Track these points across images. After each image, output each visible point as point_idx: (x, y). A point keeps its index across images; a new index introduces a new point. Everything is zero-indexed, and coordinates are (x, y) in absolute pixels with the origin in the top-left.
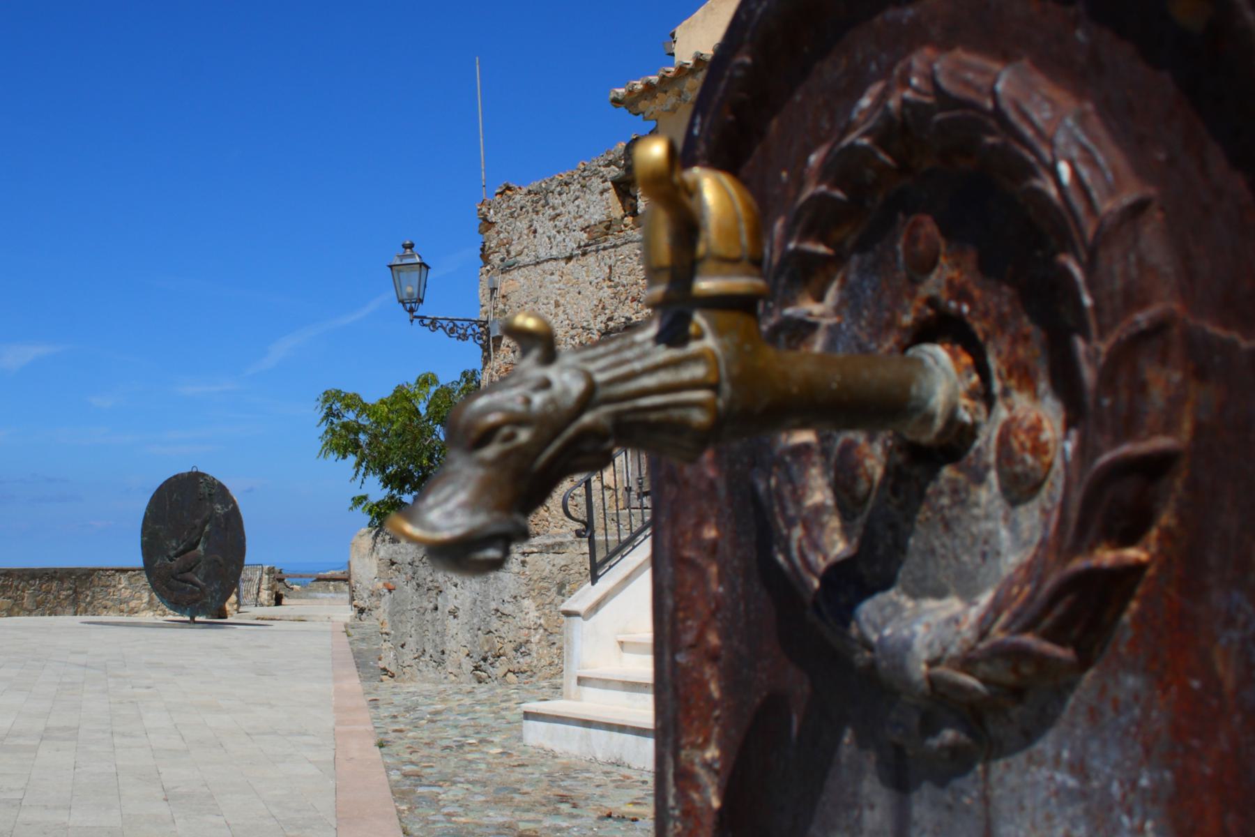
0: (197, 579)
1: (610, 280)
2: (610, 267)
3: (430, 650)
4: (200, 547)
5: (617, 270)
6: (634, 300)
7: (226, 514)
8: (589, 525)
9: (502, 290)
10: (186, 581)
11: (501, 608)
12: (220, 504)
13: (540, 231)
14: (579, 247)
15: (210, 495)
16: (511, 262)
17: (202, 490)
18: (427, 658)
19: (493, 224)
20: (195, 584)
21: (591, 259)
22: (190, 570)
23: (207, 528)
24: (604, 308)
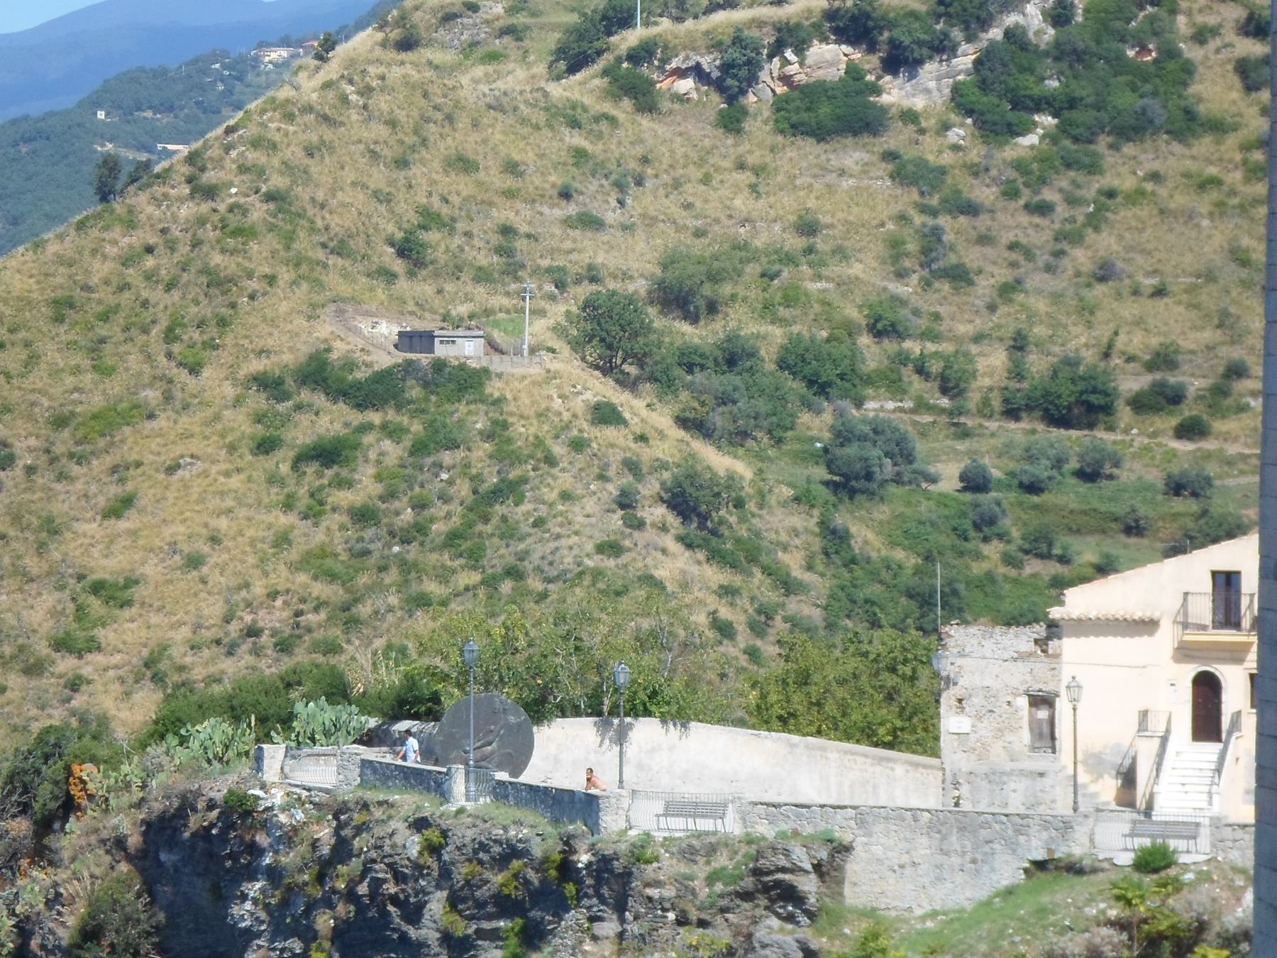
21: (1019, 663)
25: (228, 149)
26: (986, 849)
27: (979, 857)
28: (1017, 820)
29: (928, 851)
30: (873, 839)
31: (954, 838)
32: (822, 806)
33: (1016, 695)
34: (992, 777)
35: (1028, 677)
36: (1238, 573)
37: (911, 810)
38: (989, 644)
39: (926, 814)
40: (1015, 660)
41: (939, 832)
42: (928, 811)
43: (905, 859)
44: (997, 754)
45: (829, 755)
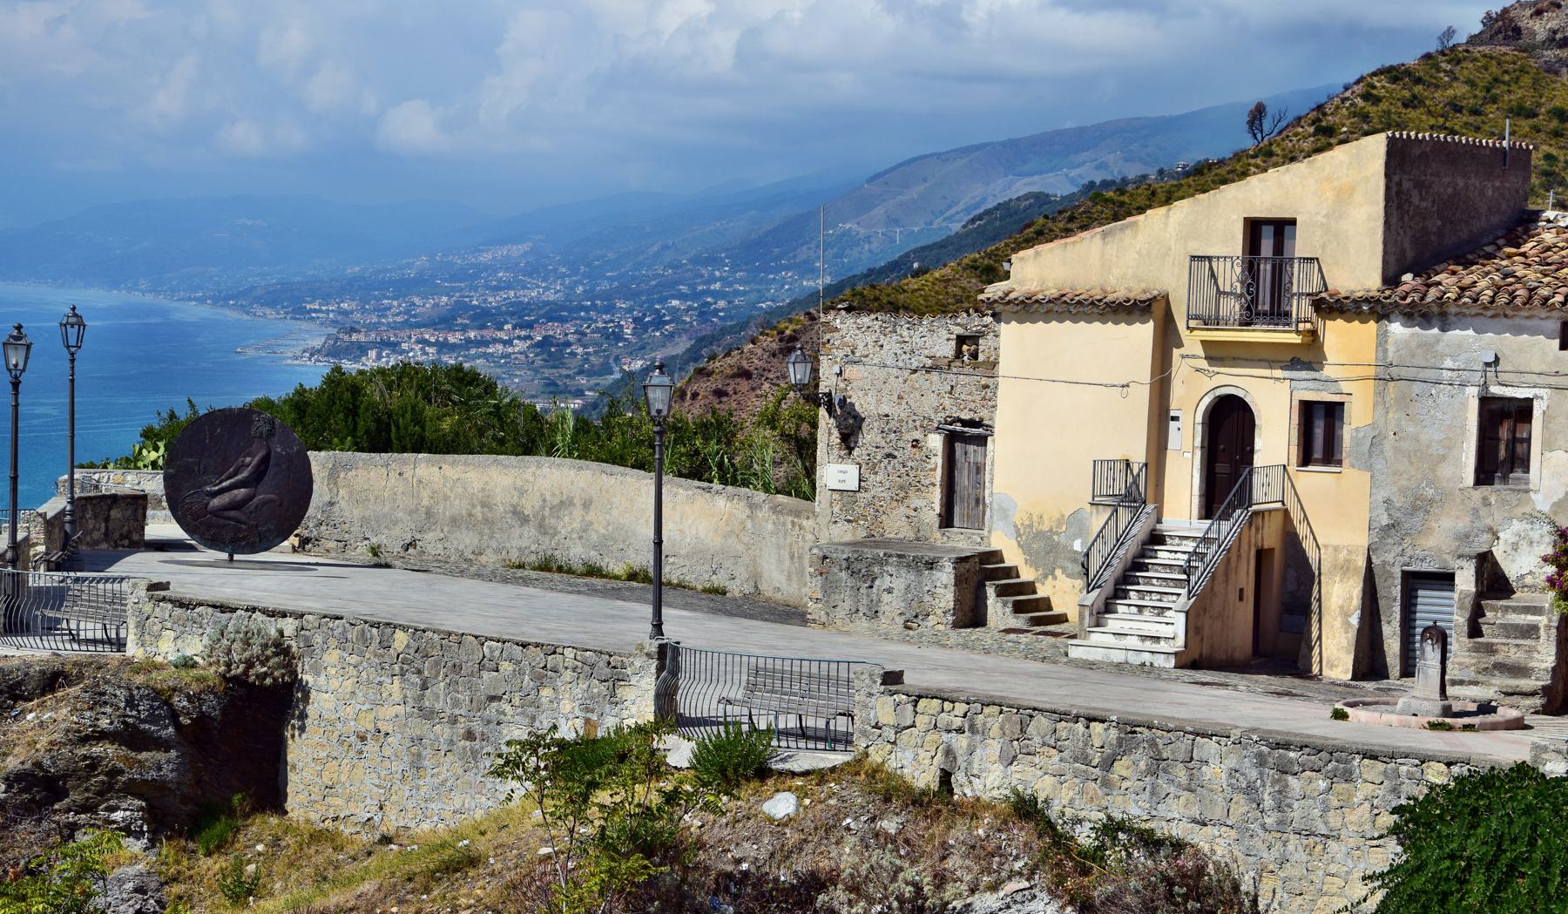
1: (951, 393)
2: (952, 387)
3: (863, 609)
5: (958, 390)
6: (970, 410)
8: (1087, 570)
9: (846, 375)
10: (229, 518)
11: (933, 590)
14: (924, 367)
16: (857, 359)
19: (836, 329)
20: (239, 521)
21: (935, 376)
24: (944, 409)
25: (1344, 100)
27: (478, 727)
29: (400, 709)
33: (926, 431)
35: (947, 402)
36: (1293, 222)
38: (891, 344)
40: (929, 370)
41: (419, 672)
42: (404, 628)
43: (366, 725)
44: (896, 526)
45: (805, 523)
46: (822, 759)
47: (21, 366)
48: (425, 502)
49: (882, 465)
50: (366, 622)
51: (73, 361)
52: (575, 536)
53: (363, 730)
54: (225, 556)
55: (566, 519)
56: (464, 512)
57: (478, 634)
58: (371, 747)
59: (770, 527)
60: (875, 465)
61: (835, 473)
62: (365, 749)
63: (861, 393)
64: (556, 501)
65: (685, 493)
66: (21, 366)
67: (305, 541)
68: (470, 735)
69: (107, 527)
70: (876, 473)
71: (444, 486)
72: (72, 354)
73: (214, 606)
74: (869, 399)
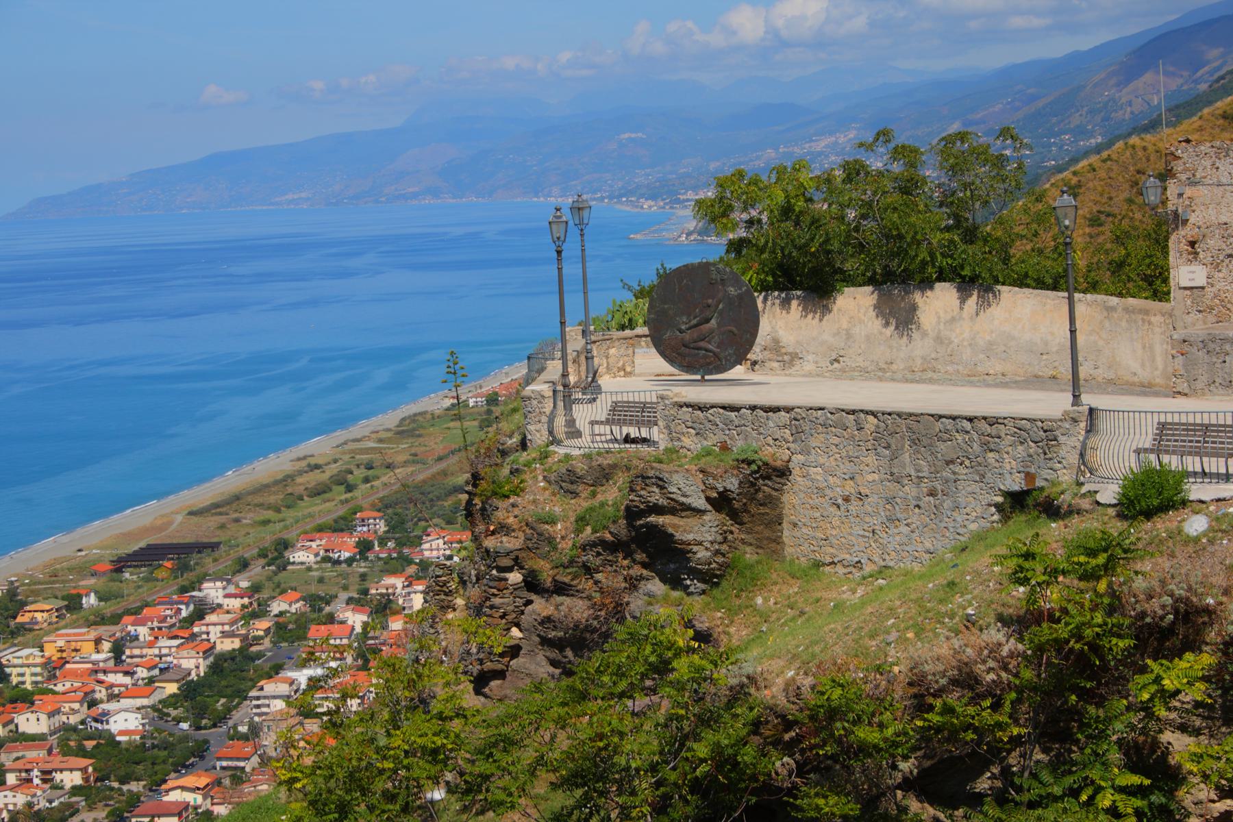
0: (710, 347)
3: (1218, 380)
4: (713, 322)
7: (739, 294)
10: (699, 349)
12: (733, 286)
13: (1222, 168)
15: (722, 280)
17: (714, 277)
18: (1217, 384)
19: (1179, 158)
22: (703, 340)
23: (721, 306)
26: (946, 474)
28: (983, 426)
29: (876, 476)
30: (812, 458)
31: (906, 457)
32: (753, 408)
34: (1211, 346)
37: (853, 412)
39: (870, 418)
41: (888, 447)
42: (874, 414)
43: (850, 488)
45: (1153, 319)
46: (1225, 490)
47: (562, 238)
48: (845, 326)
49: (1224, 264)
50: (843, 410)
51: (582, 235)
52: (965, 343)
53: (847, 493)
54: (699, 377)
55: (958, 331)
56: (876, 331)
57: (933, 412)
58: (854, 507)
59: (1124, 324)
60: (1218, 264)
61: (1185, 274)
62: (851, 508)
63: (1202, 208)
64: (949, 317)
65: (1052, 302)
66: (562, 238)
67: (754, 363)
68: (932, 493)
69: (608, 363)
70: (1219, 271)
71: (859, 312)
72: (582, 230)
73: (724, 408)
74: (1210, 211)
